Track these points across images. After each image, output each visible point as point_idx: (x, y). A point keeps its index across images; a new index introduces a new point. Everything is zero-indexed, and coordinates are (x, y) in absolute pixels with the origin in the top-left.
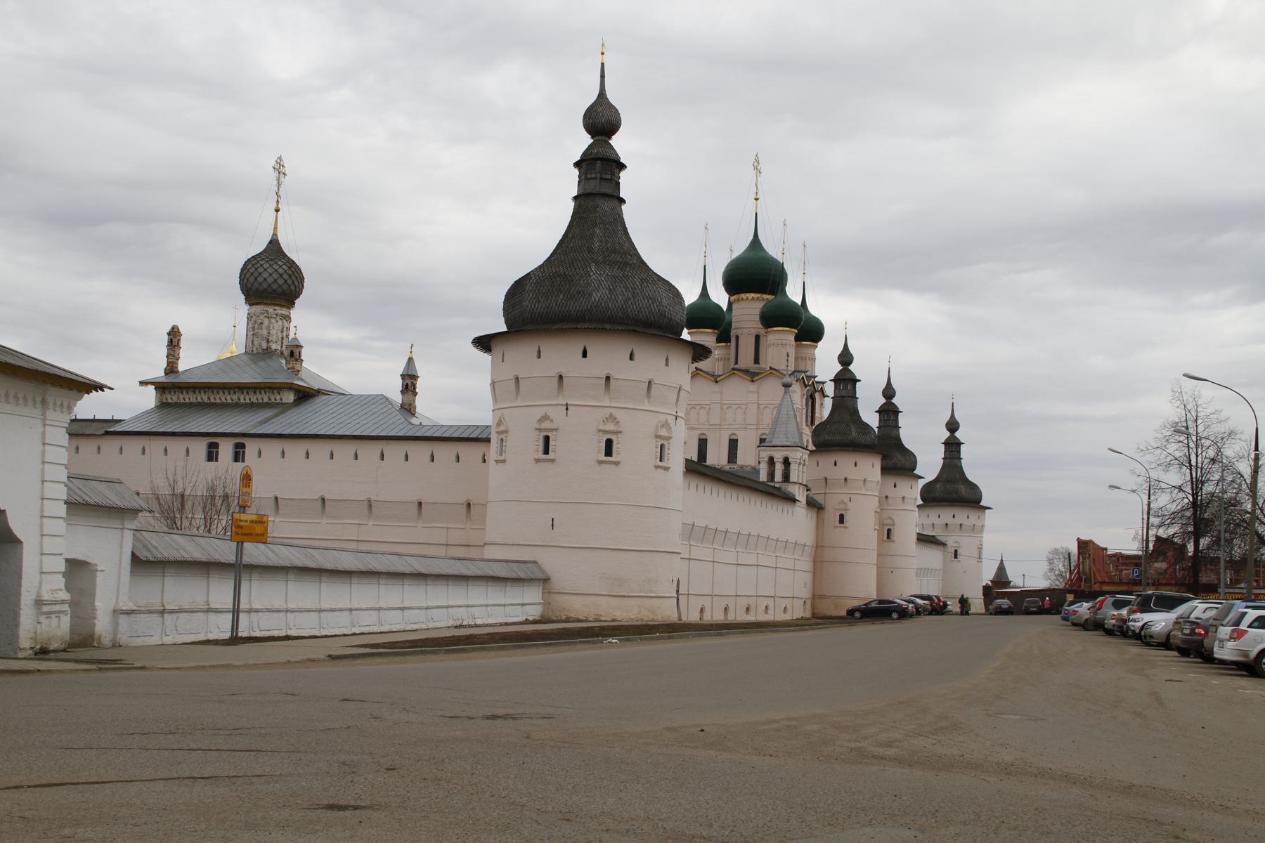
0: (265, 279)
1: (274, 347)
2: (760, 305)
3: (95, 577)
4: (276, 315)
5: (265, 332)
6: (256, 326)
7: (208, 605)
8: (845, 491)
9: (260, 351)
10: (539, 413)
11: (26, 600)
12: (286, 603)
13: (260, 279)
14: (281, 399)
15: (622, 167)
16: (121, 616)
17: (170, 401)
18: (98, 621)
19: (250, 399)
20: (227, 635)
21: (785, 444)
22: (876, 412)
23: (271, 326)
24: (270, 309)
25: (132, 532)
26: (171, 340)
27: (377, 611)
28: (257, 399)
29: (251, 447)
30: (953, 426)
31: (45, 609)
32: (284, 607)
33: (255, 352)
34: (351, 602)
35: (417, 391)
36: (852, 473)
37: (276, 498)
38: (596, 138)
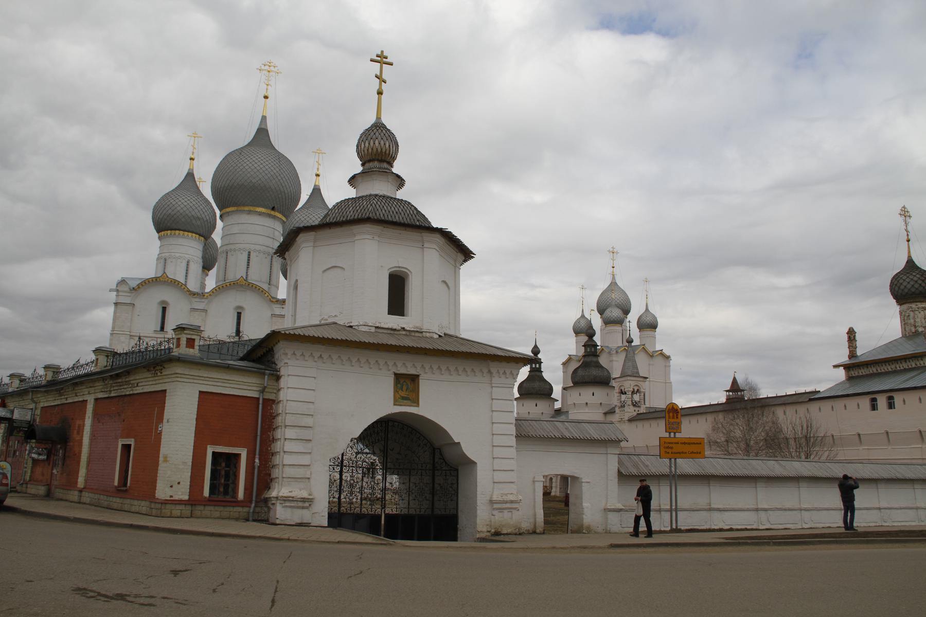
0: (905, 287)
3: (581, 487)
4: (918, 308)
5: (912, 321)
6: (906, 318)
7: (710, 506)
9: (911, 334)
12: (800, 504)
13: (902, 287)
14: (924, 363)
16: (609, 513)
17: (854, 375)
18: (586, 516)
19: (903, 367)
20: (669, 529)
23: (916, 316)
24: (913, 305)
25: (617, 456)
27: (915, 510)
28: (908, 366)
29: (898, 398)
31: (496, 506)
32: (797, 506)
33: (908, 335)
34: (879, 503)
37: (920, 431)
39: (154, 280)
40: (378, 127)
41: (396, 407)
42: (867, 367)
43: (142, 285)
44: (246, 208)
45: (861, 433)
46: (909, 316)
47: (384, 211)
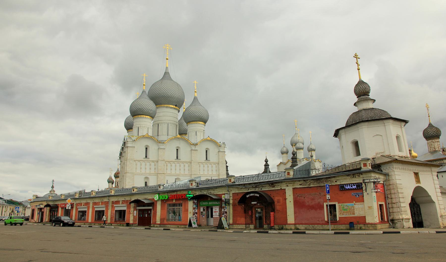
5: (433, 146)
6: (431, 145)
24: (433, 140)
39: (143, 136)
40: (361, 83)
41: (417, 184)
43: (138, 139)
44: (166, 106)
47: (372, 113)
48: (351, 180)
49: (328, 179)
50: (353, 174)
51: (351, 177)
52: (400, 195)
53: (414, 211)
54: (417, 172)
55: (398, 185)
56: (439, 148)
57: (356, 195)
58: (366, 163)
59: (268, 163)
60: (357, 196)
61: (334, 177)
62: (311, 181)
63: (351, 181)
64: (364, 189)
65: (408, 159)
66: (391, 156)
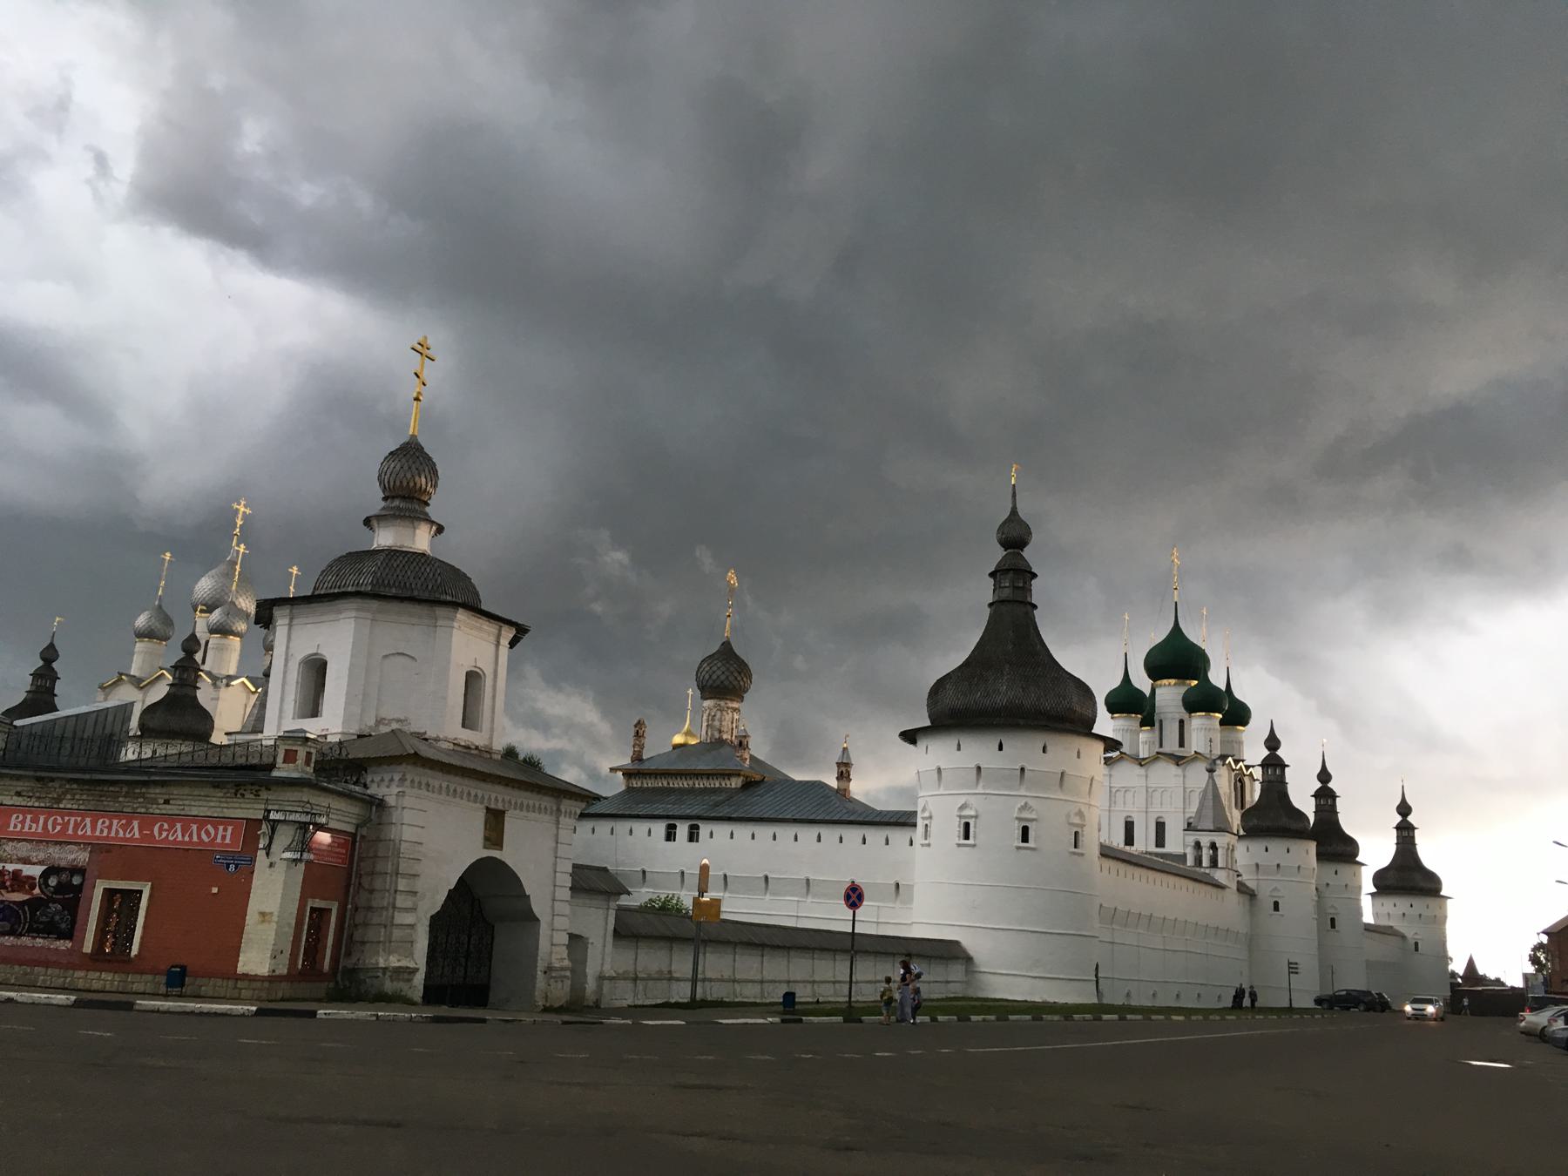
0: (718, 677)
1: (725, 737)
2: (1183, 690)
8: (1278, 877)
10: (962, 800)
11: (541, 966)
13: (714, 677)
15: (1034, 576)
21: (1212, 828)
22: (1312, 796)
24: (722, 703)
26: (638, 731)
29: (705, 829)
30: (1404, 809)
35: (851, 777)
36: (1288, 861)
37: (725, 876)
38: (1009, 551)
42: (656, 778)
45: (647, 869)
46: (715, 716)
48: (225, 805)
49: (137, 788)
50: (238, 785)
51: (225, 793)
52: (402, 884)
53: (468, 946)
54: (500, 807)
55: (404, 846)
56: (732, 733)
57: (228, 866)
58: (297, 751)
59: (55, 665)
60: (232, 867)
61: (163, 784)
62: (67, 786)
63: (225, 810)
64: (261, 846)
65: (491, 758)
66: (426, 740)
